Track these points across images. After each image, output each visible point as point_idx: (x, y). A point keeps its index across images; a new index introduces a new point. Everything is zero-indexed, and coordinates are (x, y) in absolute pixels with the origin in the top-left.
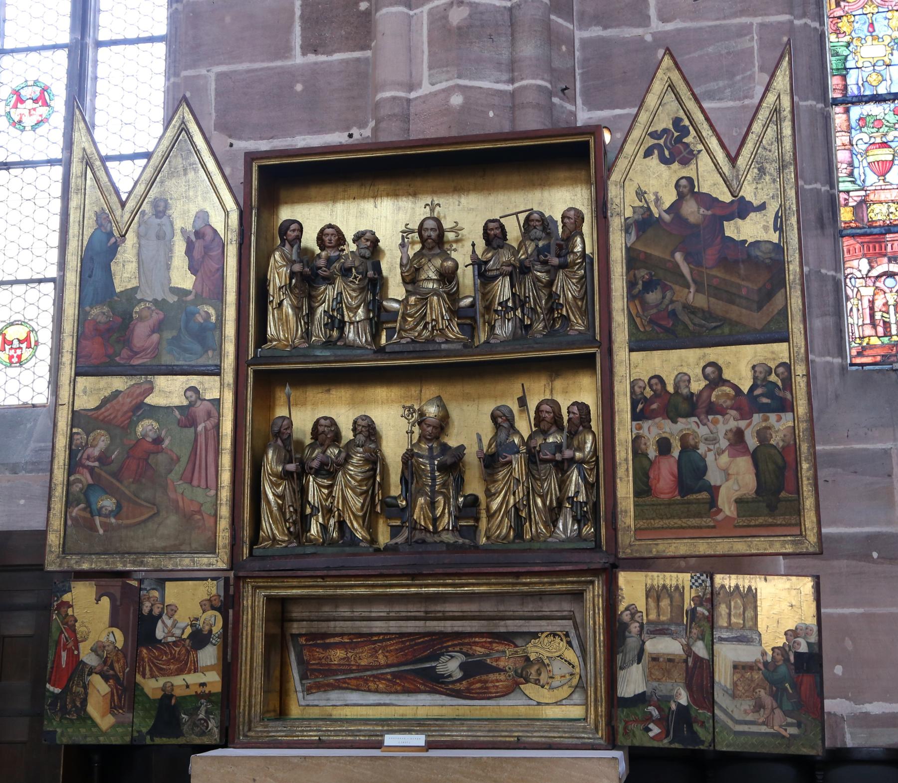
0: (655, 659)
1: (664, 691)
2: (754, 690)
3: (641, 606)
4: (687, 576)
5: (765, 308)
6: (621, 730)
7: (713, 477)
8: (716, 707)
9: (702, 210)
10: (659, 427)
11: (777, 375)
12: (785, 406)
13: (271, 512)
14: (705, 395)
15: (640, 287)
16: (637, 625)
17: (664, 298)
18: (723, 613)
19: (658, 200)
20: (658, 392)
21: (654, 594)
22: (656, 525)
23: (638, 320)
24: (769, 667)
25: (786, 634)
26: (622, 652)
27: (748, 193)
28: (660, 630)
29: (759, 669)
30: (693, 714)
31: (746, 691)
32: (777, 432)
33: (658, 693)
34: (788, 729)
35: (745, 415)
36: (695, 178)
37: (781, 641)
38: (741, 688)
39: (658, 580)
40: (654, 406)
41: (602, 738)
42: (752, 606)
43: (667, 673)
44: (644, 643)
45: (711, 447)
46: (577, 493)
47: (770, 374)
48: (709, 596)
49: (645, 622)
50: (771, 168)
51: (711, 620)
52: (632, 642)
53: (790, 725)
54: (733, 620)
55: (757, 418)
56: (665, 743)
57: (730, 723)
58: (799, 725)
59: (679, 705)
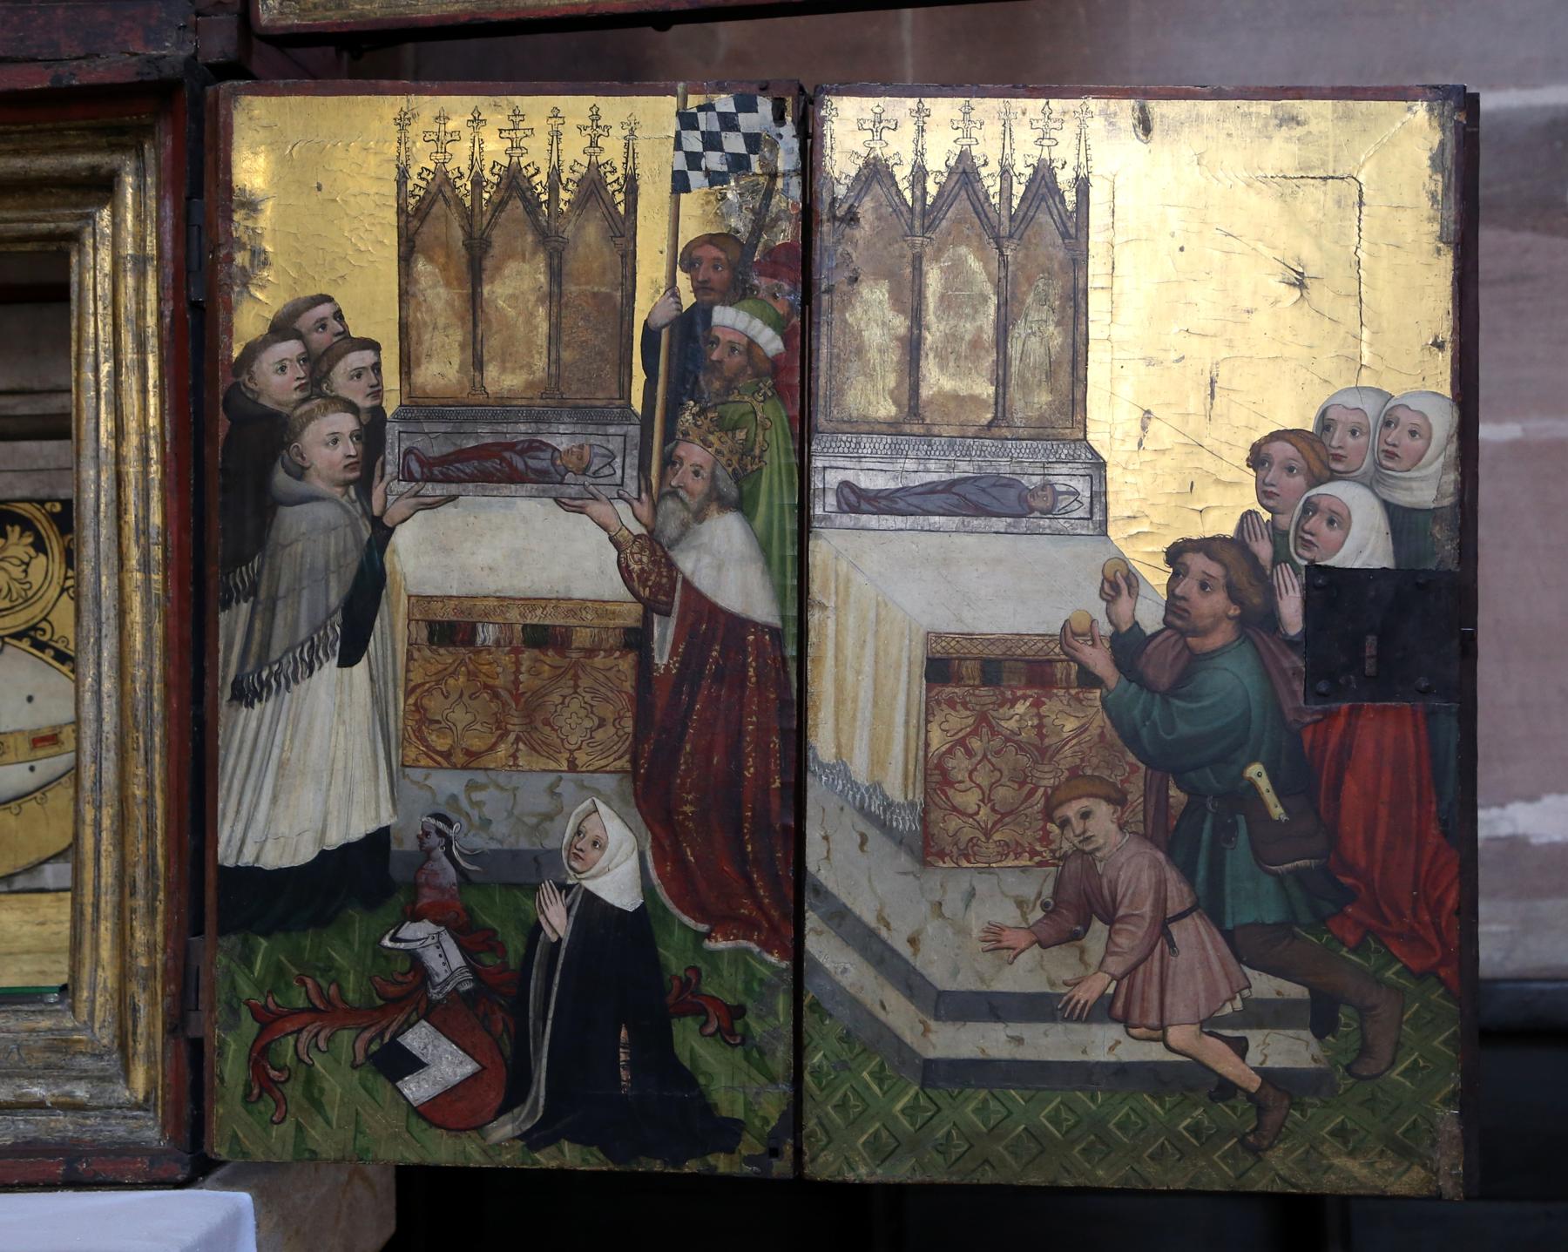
0: (449, 629)
1: (500, 828)
2: (1048, 815)
3: (371, 307)
4: (655, 114)
6: (232, 1069)
8: (812, 920)
16: (345, 423)
18: (874, 336)
21: (449, 229)
24: (1144, 666)
25: (1258, 457)
26: (253, 590)
28: (482, 452)
29: (1089, 679)
30: (674, 962)
31: (1004, 815)
33: (469, 839)
34: (1255, 1037)
37: (1227, 506)
38: (970, 800)
39: (477, 142)
41: (145, 1105)
42: (1057, 288)
43: (524, 717)
44: (382, 533)
48: (786, 233)
49: (391, 404)
51: (797, 380)
52: (312, 532)
54: (936, 380)
56: (501, 1139)
57: (900, 1015)
58: (1321, 1017)
59: (591, 910)
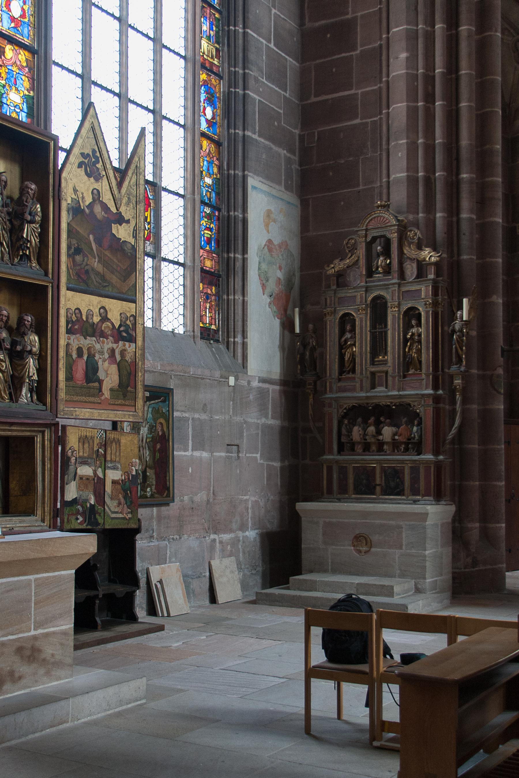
0: (81, 478)
5: (127, 281)
6: (66, 520)
7: (101, 374)
9: (103, 213)
10: (79, 341)
11: (130, 321)
12: (132, 339)
14: (100, 325)
15: (73, 250)
17: (83, 261)
19: (83, 198)
20: (79, 319)
22: (74, 399)
23: (71, 271)
27: (123, 209)
30: (96, 509)
32: (128, 353)
35: (116, 342)
36: (101, 191)
40: (76, 327)
41: (47, 526)
43: (86, 487)
44: (77, 469)
45: (101, 356)
46: (34, 374)
47: (127, 320)
48: (104, 443)
50: (133, 200)
52: (72, 468)
53: (129, 513)
55: (121, 343)
57: (110, 513)
58: (131, 513)
59: (91, 504)
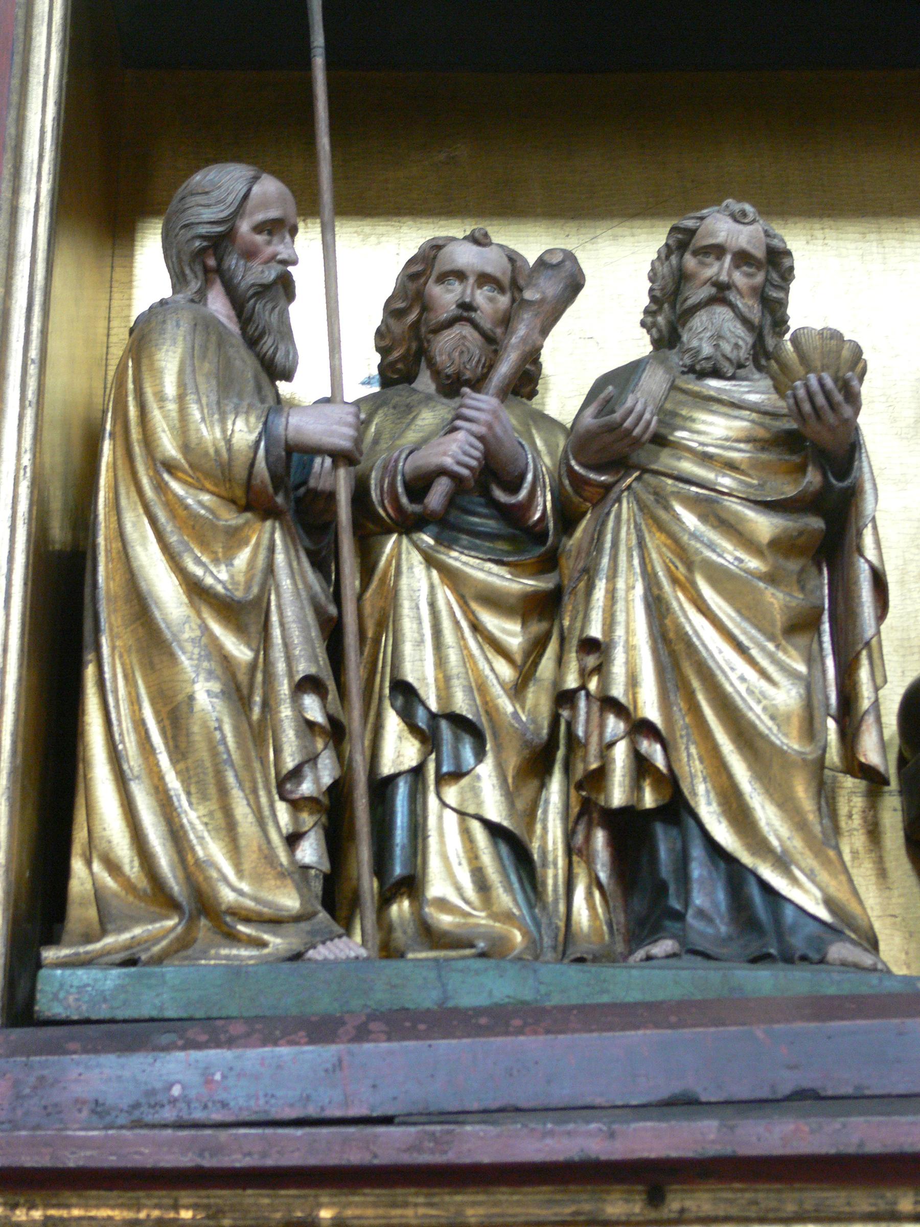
13: (175, 715)
